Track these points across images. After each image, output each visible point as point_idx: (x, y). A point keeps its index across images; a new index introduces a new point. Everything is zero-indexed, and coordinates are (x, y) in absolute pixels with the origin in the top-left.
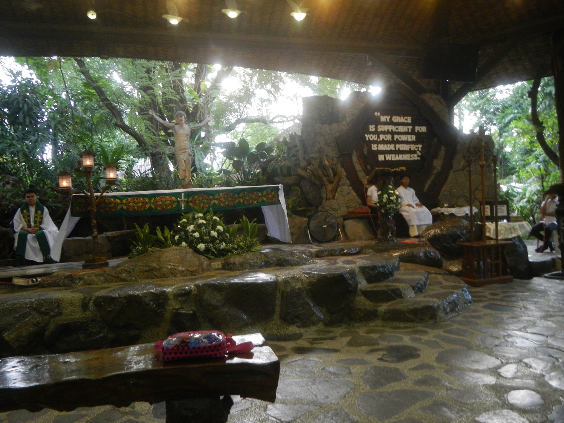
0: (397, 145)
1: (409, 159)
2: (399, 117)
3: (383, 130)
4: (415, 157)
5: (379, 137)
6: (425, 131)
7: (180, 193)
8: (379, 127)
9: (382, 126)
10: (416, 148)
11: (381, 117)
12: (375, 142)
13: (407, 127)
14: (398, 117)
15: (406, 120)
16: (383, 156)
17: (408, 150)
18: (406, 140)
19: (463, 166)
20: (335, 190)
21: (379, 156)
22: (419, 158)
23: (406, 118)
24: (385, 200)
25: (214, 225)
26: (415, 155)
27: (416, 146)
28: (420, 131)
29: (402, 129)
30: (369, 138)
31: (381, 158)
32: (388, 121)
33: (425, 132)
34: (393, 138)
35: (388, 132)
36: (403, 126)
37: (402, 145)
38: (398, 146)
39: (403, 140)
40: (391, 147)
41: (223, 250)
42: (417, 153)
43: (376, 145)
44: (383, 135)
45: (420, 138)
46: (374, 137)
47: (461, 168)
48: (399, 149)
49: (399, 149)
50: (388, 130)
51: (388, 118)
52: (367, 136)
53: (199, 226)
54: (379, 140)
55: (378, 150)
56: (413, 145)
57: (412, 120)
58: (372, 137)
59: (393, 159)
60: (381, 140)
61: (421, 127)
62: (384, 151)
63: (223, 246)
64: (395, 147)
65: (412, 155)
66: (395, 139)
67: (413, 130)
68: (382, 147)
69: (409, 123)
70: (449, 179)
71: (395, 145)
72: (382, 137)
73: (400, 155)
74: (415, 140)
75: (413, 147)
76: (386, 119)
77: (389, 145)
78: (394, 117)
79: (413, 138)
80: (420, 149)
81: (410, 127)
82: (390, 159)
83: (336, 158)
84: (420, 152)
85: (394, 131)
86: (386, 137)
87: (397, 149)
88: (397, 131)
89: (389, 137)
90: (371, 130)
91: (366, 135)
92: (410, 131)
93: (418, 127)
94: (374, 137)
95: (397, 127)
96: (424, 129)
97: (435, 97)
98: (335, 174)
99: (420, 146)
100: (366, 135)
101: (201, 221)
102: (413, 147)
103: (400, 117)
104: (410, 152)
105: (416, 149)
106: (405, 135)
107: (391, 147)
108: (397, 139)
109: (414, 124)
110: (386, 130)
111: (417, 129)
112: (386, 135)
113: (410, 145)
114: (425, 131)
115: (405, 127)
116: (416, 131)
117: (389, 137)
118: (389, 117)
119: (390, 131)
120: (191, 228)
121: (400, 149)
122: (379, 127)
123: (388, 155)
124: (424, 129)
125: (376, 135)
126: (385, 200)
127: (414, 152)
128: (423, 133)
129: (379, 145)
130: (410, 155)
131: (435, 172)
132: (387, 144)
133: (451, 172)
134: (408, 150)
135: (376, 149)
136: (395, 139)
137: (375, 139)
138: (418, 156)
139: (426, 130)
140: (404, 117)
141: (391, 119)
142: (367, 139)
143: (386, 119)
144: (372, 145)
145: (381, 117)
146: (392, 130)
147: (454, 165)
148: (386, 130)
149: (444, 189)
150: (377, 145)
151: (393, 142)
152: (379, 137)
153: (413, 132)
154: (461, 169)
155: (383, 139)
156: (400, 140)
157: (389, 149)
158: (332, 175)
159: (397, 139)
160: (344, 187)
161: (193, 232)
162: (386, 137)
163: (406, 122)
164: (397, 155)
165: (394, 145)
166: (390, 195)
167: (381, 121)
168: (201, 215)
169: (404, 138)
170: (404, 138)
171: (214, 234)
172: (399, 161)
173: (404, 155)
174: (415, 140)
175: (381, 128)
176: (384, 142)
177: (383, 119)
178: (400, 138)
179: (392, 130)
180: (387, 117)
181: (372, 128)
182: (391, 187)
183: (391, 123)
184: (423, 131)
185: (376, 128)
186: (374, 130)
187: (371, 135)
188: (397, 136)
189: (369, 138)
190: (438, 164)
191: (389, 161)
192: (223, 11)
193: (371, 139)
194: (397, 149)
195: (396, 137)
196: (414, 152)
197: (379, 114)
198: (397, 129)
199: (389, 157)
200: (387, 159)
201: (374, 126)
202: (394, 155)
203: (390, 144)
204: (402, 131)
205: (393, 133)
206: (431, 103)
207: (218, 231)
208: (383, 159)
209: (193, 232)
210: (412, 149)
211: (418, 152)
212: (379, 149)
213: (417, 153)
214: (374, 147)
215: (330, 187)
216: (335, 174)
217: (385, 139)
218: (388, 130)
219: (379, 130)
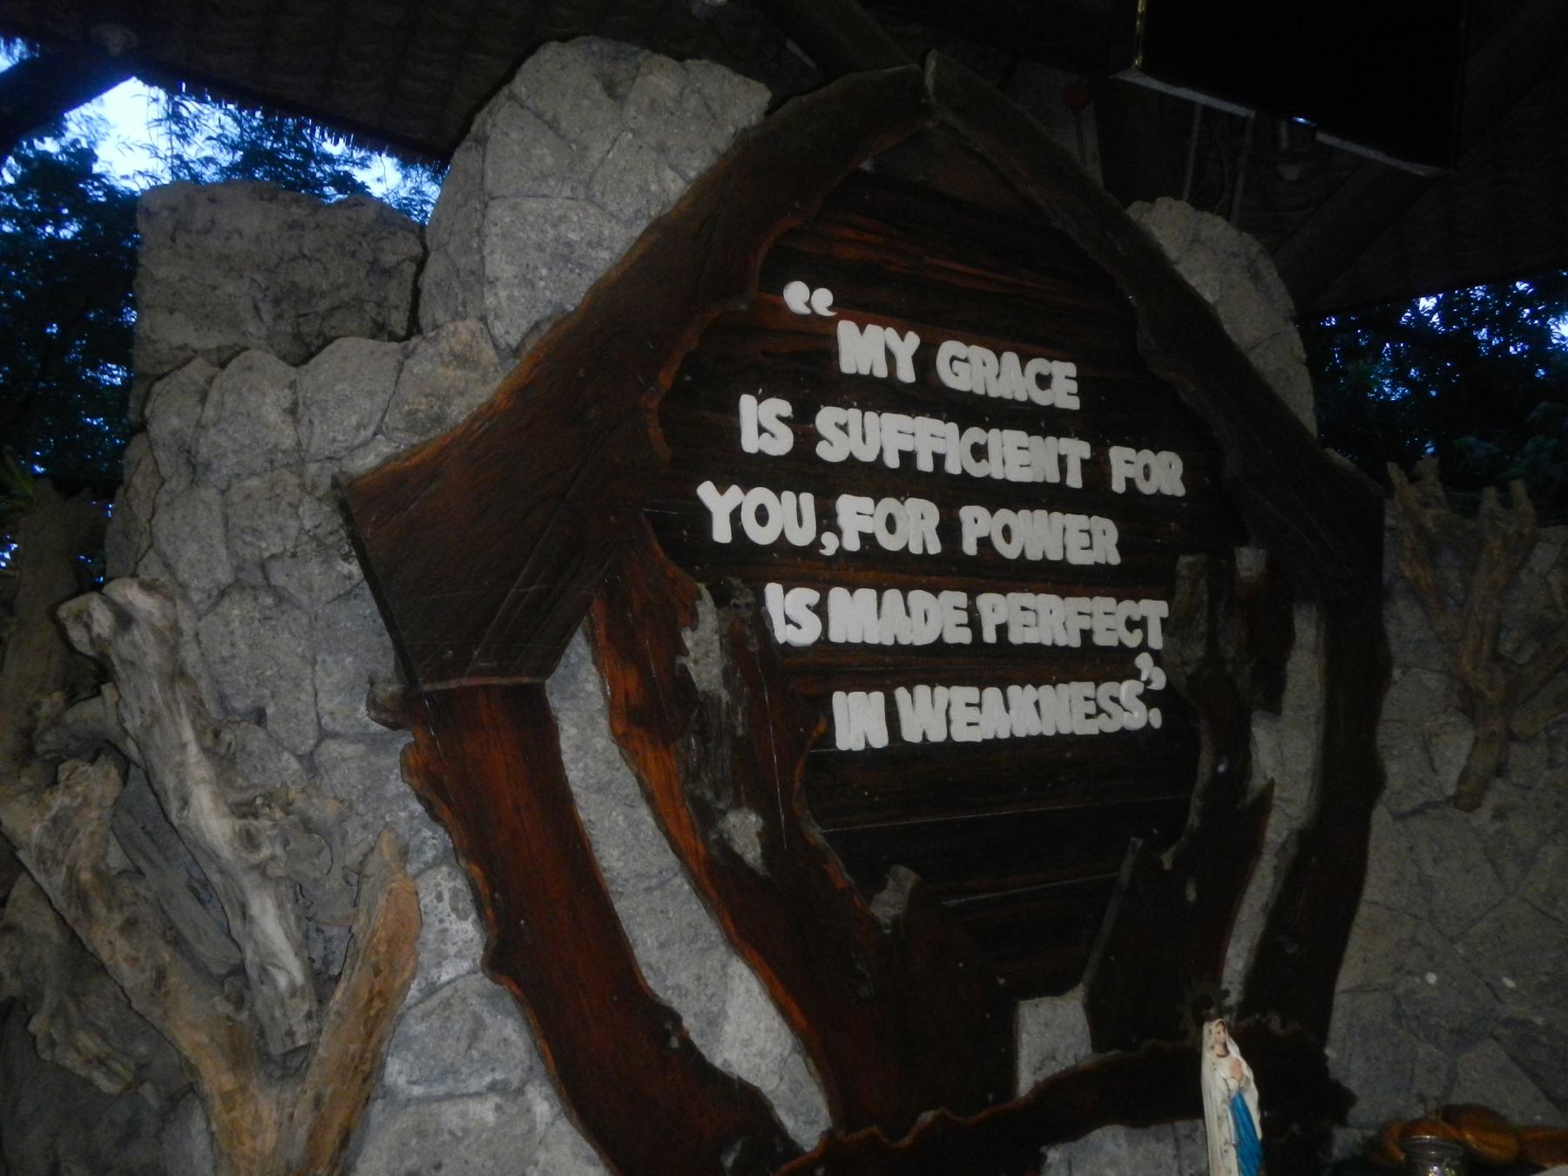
0: (986, 601)
1: (1091, 728)
2: (989, 355)
3: (867, 455)
5: (827, 519)
6: (1180, 491)
8: (827, 418)
9: (853, 415)
10: (1131, 625)
11: (846, 330)
13: (1051, 440)
14: (979, 353)
15: (1044, 381)
16: (878, 697)
17: (1075, 642)
18: (1055, 555)
19: (1464, 777)
21: (838, 698)
22: (1156, 718)
23: (1038, 365)
26: (1128, 690)
27: (1130, 608)
28: (1147, 488)
30: (735, 516)
32: (907, 374)
33: (1173, 498)
34: (949, 530)
36: (1019, 437)
37: (1027, 599)
38: (996, 608)
39: (1034, 554)
42: (1136, 674)
44: (866, 503)
47: (1451, 791)
48: (1002, 630)
49: (1002, 630)
50: (908, 457)
51: (907, 346)
54: (830, 544)
55: (824, 641)
56: (1108, 603)
57: (1085, 384)
58: (762, 516)
59: (962, 734)
60: (852, 544)
61: (1146, 456)
62: (880, 648)
64: (974, 623)
65: (1108, 688)
66: (970, 547)
67: (1096, 469)
69: (1066, 413)
70: (1376, 887)
71: (972, 599)
73: (1014, 690)
74: (1115, 559)
76: (890, 357)
77: (919, 598)
78: (949, 348)
80: (1156, 640)
81: (1077, 450)
82: (937, 735)
83: (362, 737)
84: (1158, 658)
85: (952, 467)
86: (891, 524)
87: (990, 636)
88: (977, 470)
90: (750, 442)
91: (706, 491)
92: (1075, 480)
93: (1129, 452)
95: (975, 434)
97: (1217, 228)
99: (1155, 610)
100: (706, 491)
103: (999, 355)
105: (1133, 640)
106: (1041, 514)
108: (984, 543)
110: (893, 461)
111: (1124, 464)
112: (889, 504)
113: (1083, 603)
114: (1180, 491)
115: (1037, 439)
116: (1118, 486)
118: (913, 340)
119: (925, 464)
121: (1016, 637)
122: (827, 418)
123: (922, 691)
125: (807, 499)
129: (838, 595)
130: (1087, 688)
131: (1278, 830)
132: (905, 591)
133: (1380, 816)
134: (1075, 642)
135: (806, 634)
136: (970, 547)
137: (801, 537)
138: (1149, 698)
139: (1185, 479)
140: (1024, 360)
141: (924, 360)
142: (722, 533)
143: (890, 357)
144: (773, 591)
145: (846, 329)
146: (939, 459)
147: (1393, 768)
148: (893, 461)
149: (1346, 979)
150: (813, 596)
152: (827, 519)
154: (1455, 800)
155: (867, 539)
156: (1010, 551)
157: (920, 635)
158: (290, 970)
159: (984, 543)
160: (450, 1115)
162: (891, 524)
163: (1042, 398)
164: (992, 694)
165: (961, 598)
167: (847, 366)
172: (1013, 741)
173: (1046, 690)
174: (1115, 559)
178: (1007, 532)
179: (939, 459)
180: (891, 334)
184: (1167, 491)
186: (781, 443)
187: (761, 495)
188: (979, 511)
189: (735, 516)
191: (926, 747)
193: (762, 536)
194: (990, 636)
195: (976, 523)
197: (823, 300)
198: (979, 452)
200: (911, 734)
201: (785, 408)
202: (971, 693)
203: (936, 591)
204: (1017, 475)
206: (1203, 279)
208: (880, 740)
210: (1101, 639)
211: (1144, 662)
212: (836, 636)
213: (1136, 674)
218: (908, 457)
219: (831, 451)
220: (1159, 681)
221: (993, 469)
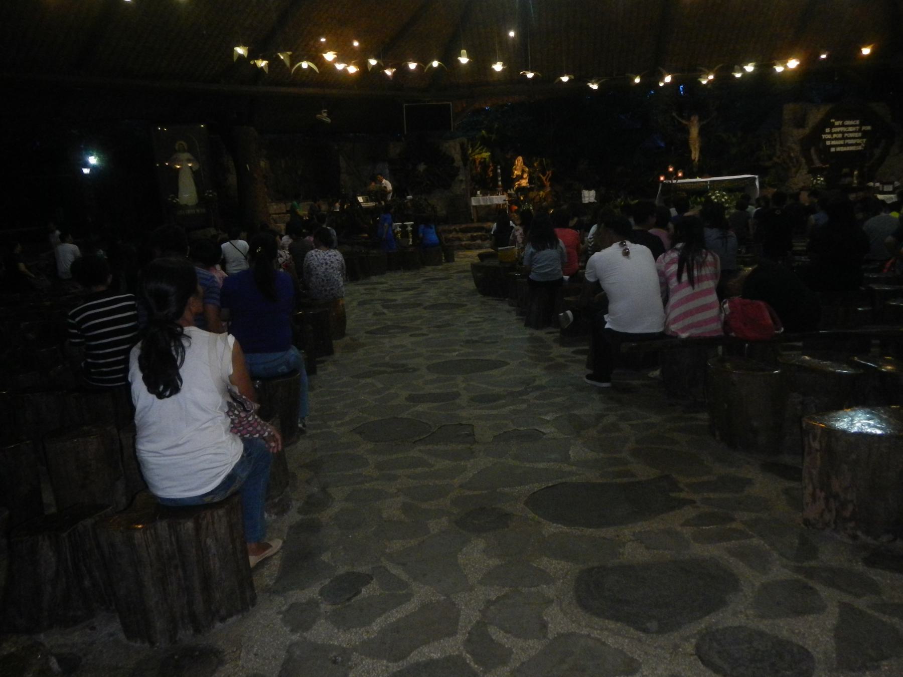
4: (860, 148)
7: (706, 182)
8: (833, 129)
12: (829, 139)
15: (855, 122)
20: (797, 172)
23: (855, 121)
24: (814, 183)
25: (723, 196)
27: (861, 140)
29: (850, 129)
31: (833, 150)
35: (840, 132)
40: (841, 142)
41: (727, 207)
43: (829, 142)
45: (865, 134)
46: (829, 136)
52: (824, 136)
53: (717, 197)
63: (727, 205)
64: (844, 142)
68: (834, 143)
72: (835, 136)
75: (859, 141)
79: (860, 135)
81: (858, 128)
84: (864, 144)
89: (840, 136)
94: (829, 136)
96: (869, 128)
98: (797, 161)
99: (865, 140)
101: (718, 195)
102: (859, 141)
104: (857, 144)
107: (841, 142)
109: (861, 125)
111: (864, 128)
117: (840, 136)
120: (713, 197)
124: (869, 128)
126: (814, 183)
127: (859, 144)
128: (868, 131)
136: (845, 136)
137: (830, 137)
138: (862, 147)
141: (843, 123)
142: (823, 138)
151: (843, 138)
152: (832, 136)
153: (860, 131)
161: (714, 199)
166: (818, 180)
168: (717, 192)
169: (852, 135)
170: (852, 135)
171: (723, 200)
175: (834, 130)
176: (836, 139)
177: (837, 123)
181: (828, 130)
182: (819, 176)
183: (843, 126)
185: (831, 130)
190: (877, 152)
192: (733, 73)
195: (846, 135)
196: (859, 144)
198: (847, 129)
199: (839, 149)
205: (843, 133)
207: (725, 199)
209: (714, 199)
214: (828, 143)
215: (794, 170)
216: (797, 161)
217: (837, 137)
220: (864, 145)
221: (848, 130)
